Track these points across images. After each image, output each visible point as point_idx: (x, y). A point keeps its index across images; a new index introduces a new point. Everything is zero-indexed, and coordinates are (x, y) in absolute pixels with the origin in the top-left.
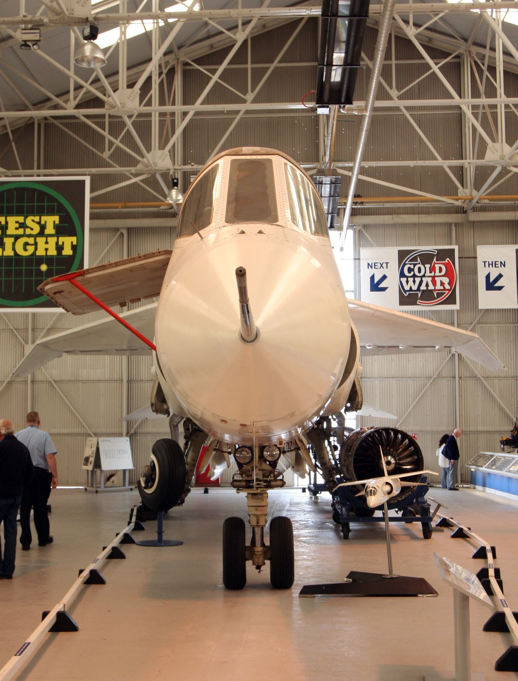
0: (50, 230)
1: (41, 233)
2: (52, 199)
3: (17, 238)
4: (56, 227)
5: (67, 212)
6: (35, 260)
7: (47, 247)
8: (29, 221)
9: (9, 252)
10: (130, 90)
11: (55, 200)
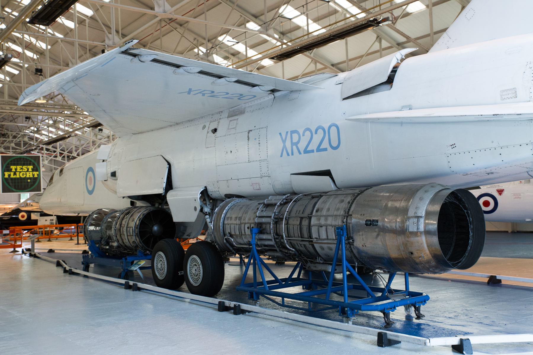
0: (30, 170)
1: (28, 171)
2: (31, 161)
3: (20, 172)
4: (32, 169)
6: (26, 179)
7: (29, 175)
8: (24, 167)
9: (18, 176)
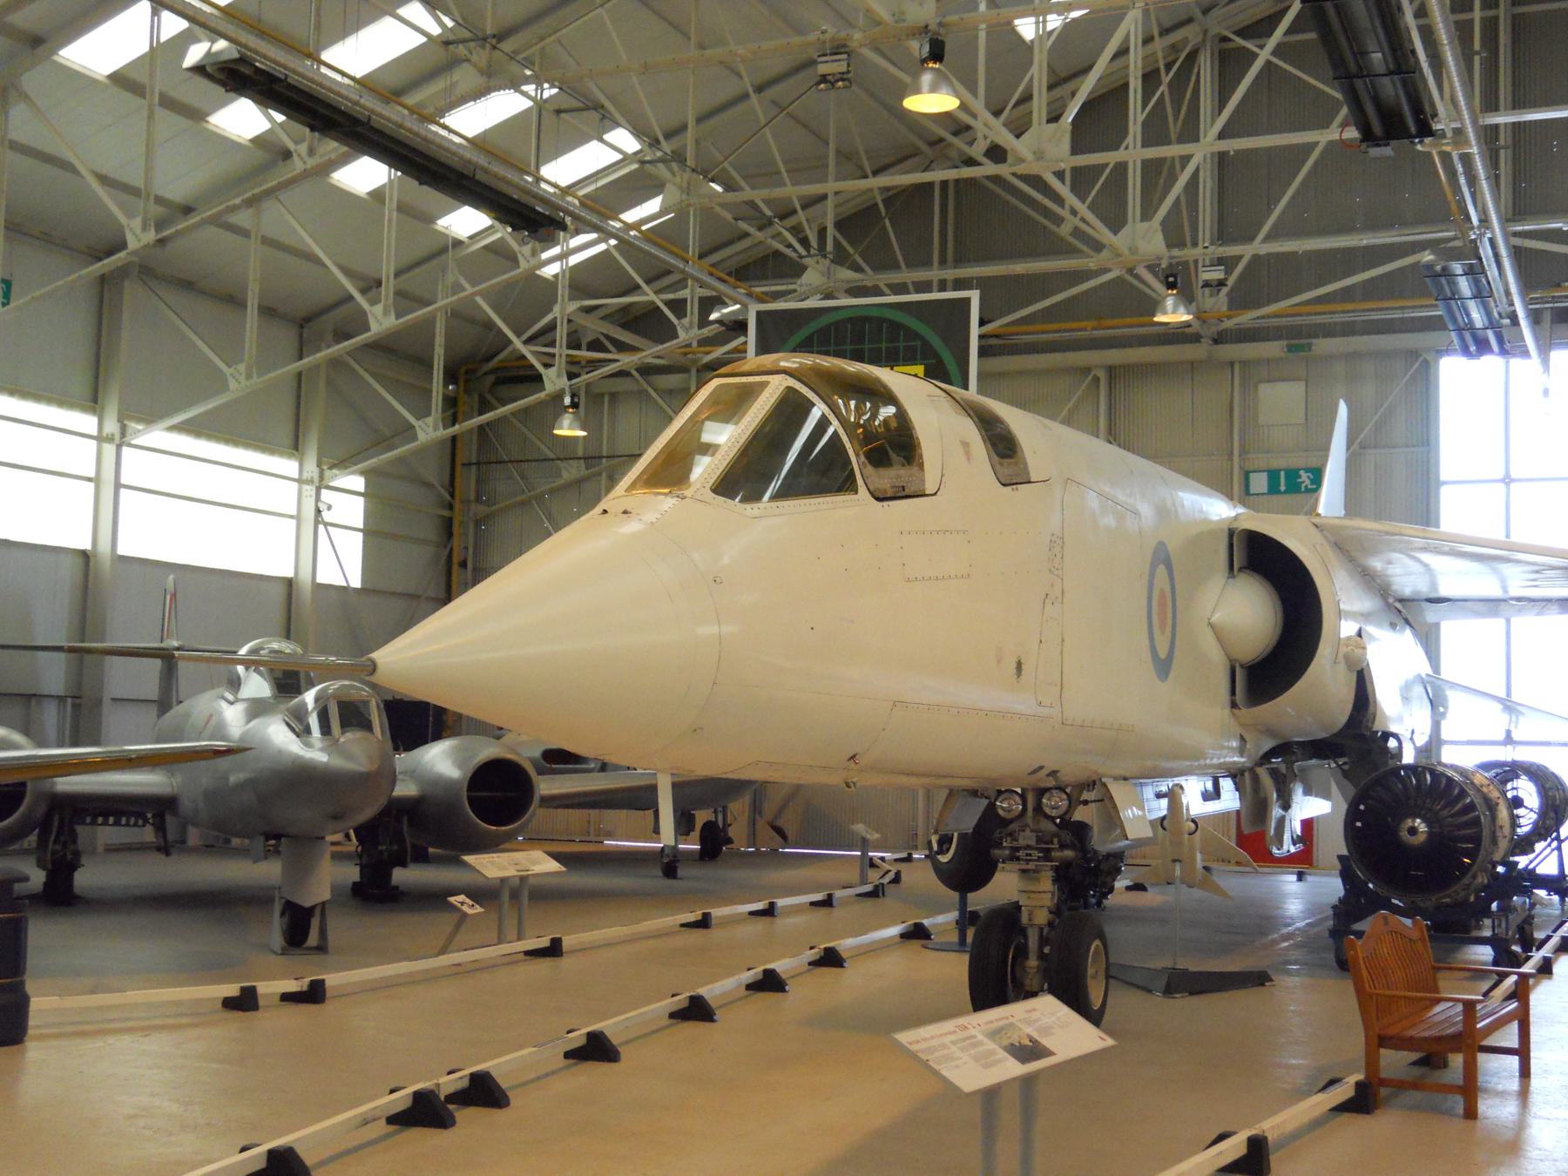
5: (936, 355)
10: (1053, 126)
11: (917, 336)
